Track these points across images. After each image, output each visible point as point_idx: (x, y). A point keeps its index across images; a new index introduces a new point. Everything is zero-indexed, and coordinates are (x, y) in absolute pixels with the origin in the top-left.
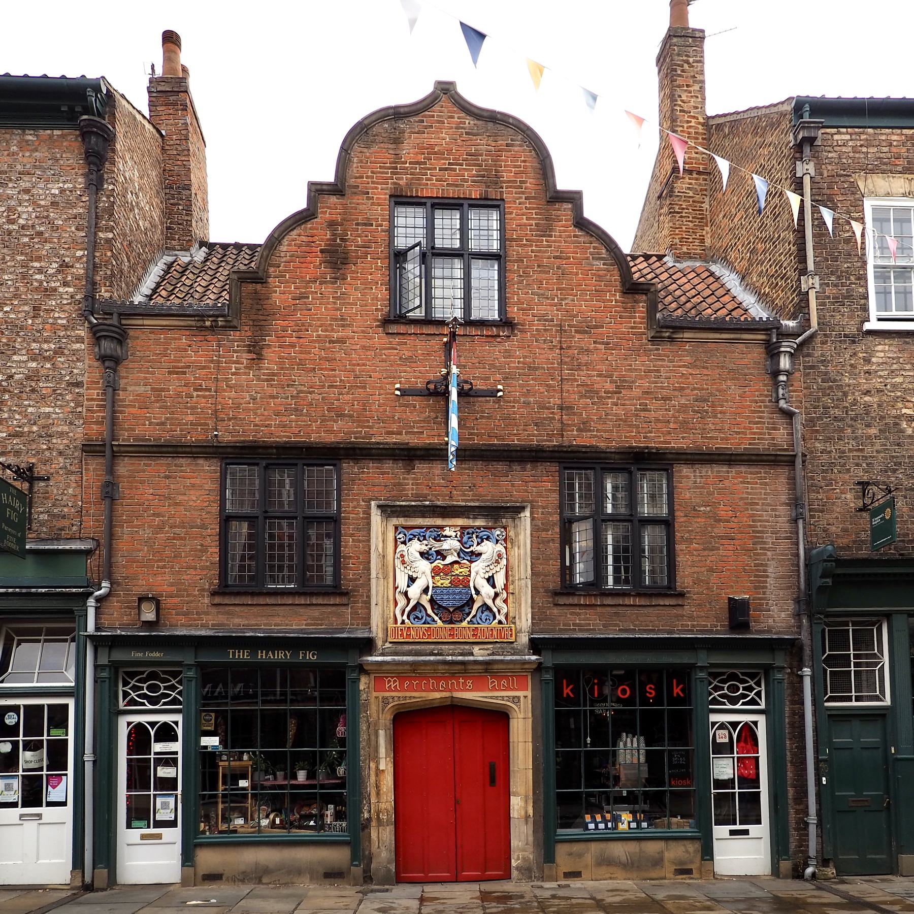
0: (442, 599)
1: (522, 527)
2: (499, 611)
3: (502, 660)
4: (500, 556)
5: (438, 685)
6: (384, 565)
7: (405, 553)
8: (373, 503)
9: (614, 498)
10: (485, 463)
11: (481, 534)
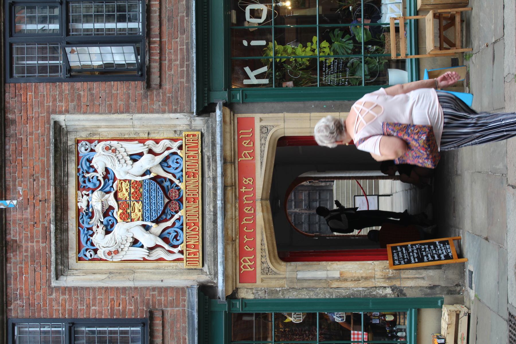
0: (156, 211)
1: (77, 123)
2: (168, 149)
3: (221, 146)
4: (107, 148)
5: (248, 215)
7: (107, 250)
8: (54, 283)
9: (43, 20)
10: (8, 163)
11: (85, 168)
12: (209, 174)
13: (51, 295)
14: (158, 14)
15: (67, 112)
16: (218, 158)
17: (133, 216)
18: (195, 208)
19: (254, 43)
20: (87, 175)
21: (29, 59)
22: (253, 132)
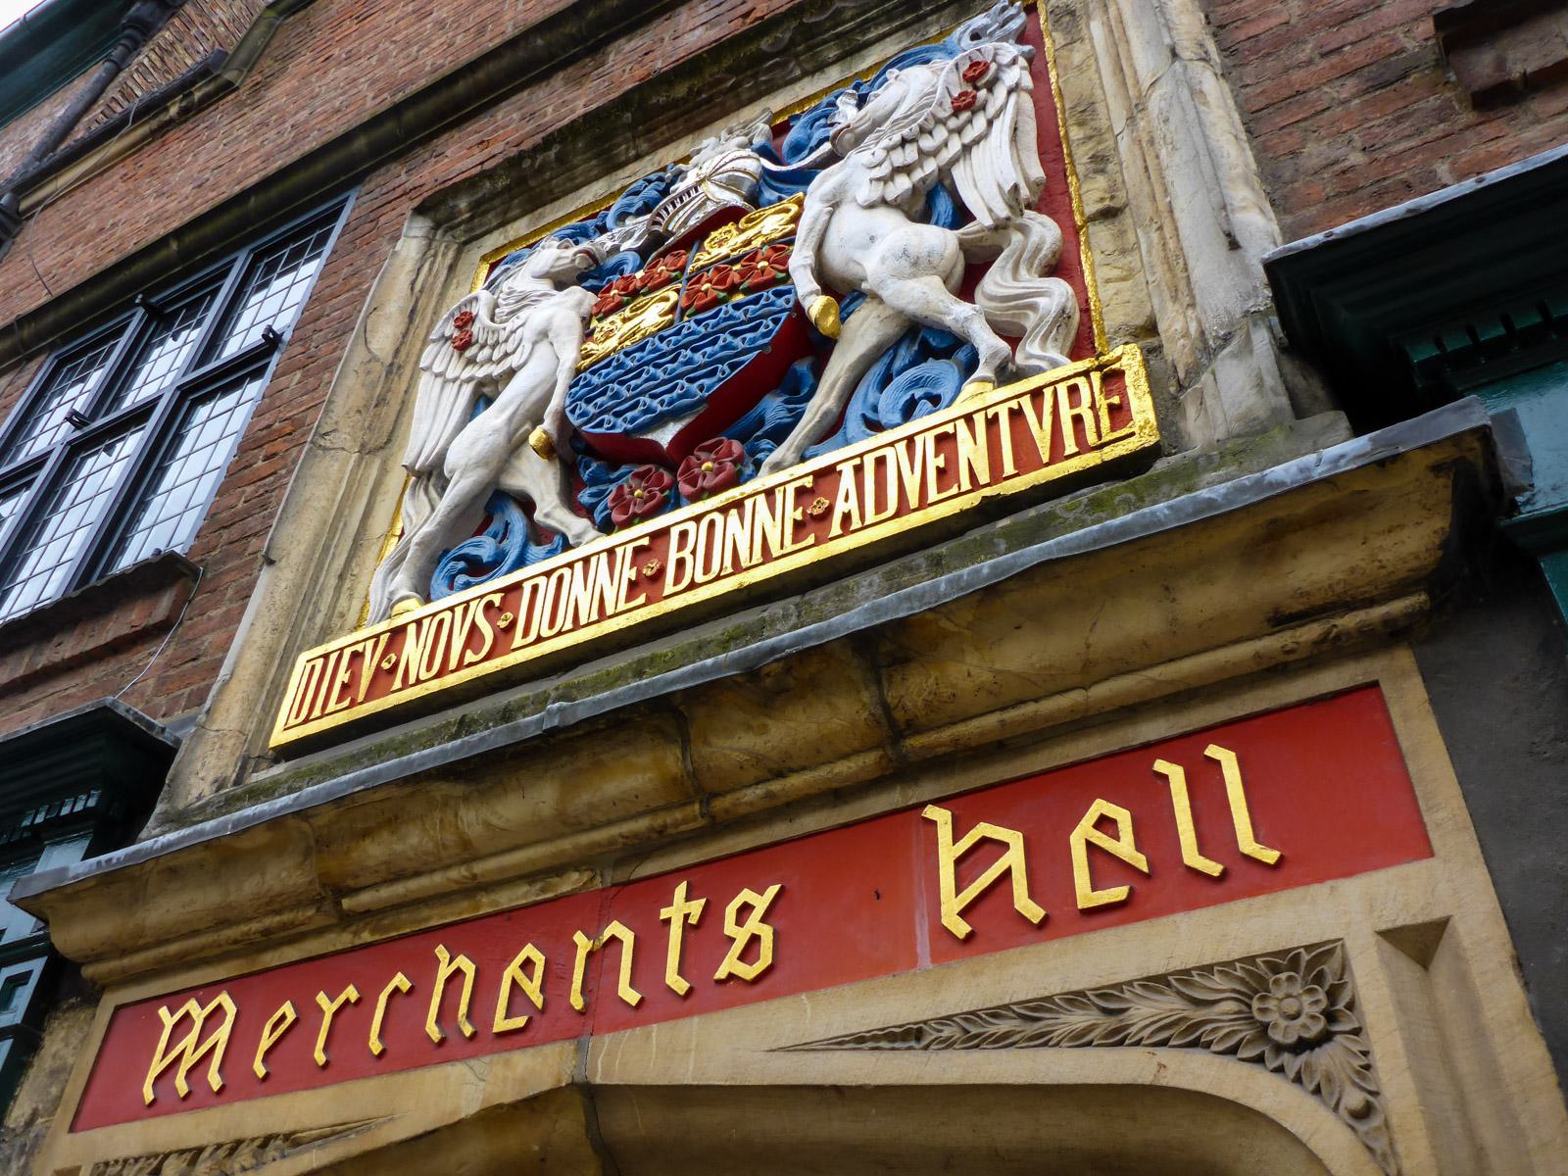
7: (481, 310)
22: (1240, 879)
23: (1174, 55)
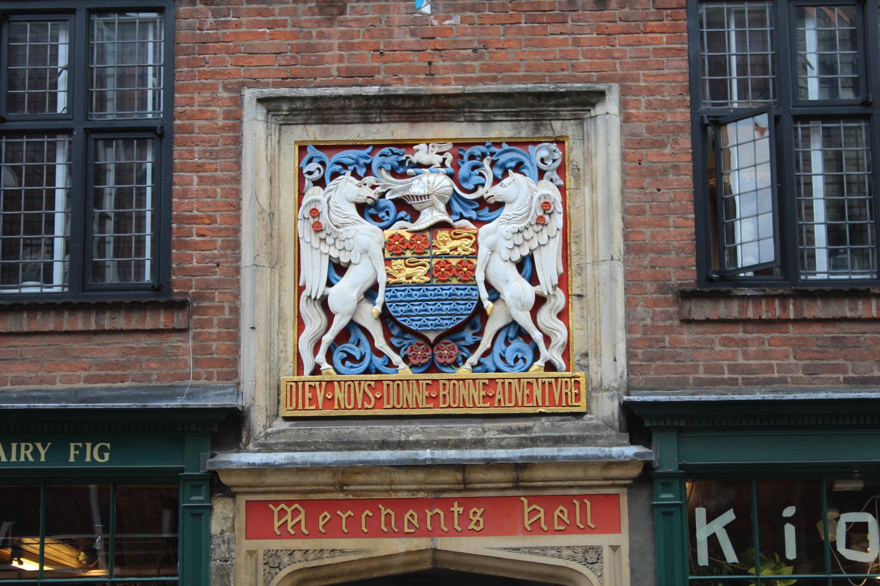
0: (408, 314)
1: (601, 140)
2: (547, 340)
3: (553, 458)
4: (546, 206)
6: (272, 236)
7: (322, 208)
8: (250, 95)
9: (827, 66)
11: (503, 159)
12: (492, 430)
13: (225, 88)
14: (849, 314)
15: (626, 119)
16: (527, 452)
17: (398, 263)
18: (415, 400)
19: (790, 531)
20: (486, 163)
21: (741, 36)
22: (587, 530)
23: (612, 258)
